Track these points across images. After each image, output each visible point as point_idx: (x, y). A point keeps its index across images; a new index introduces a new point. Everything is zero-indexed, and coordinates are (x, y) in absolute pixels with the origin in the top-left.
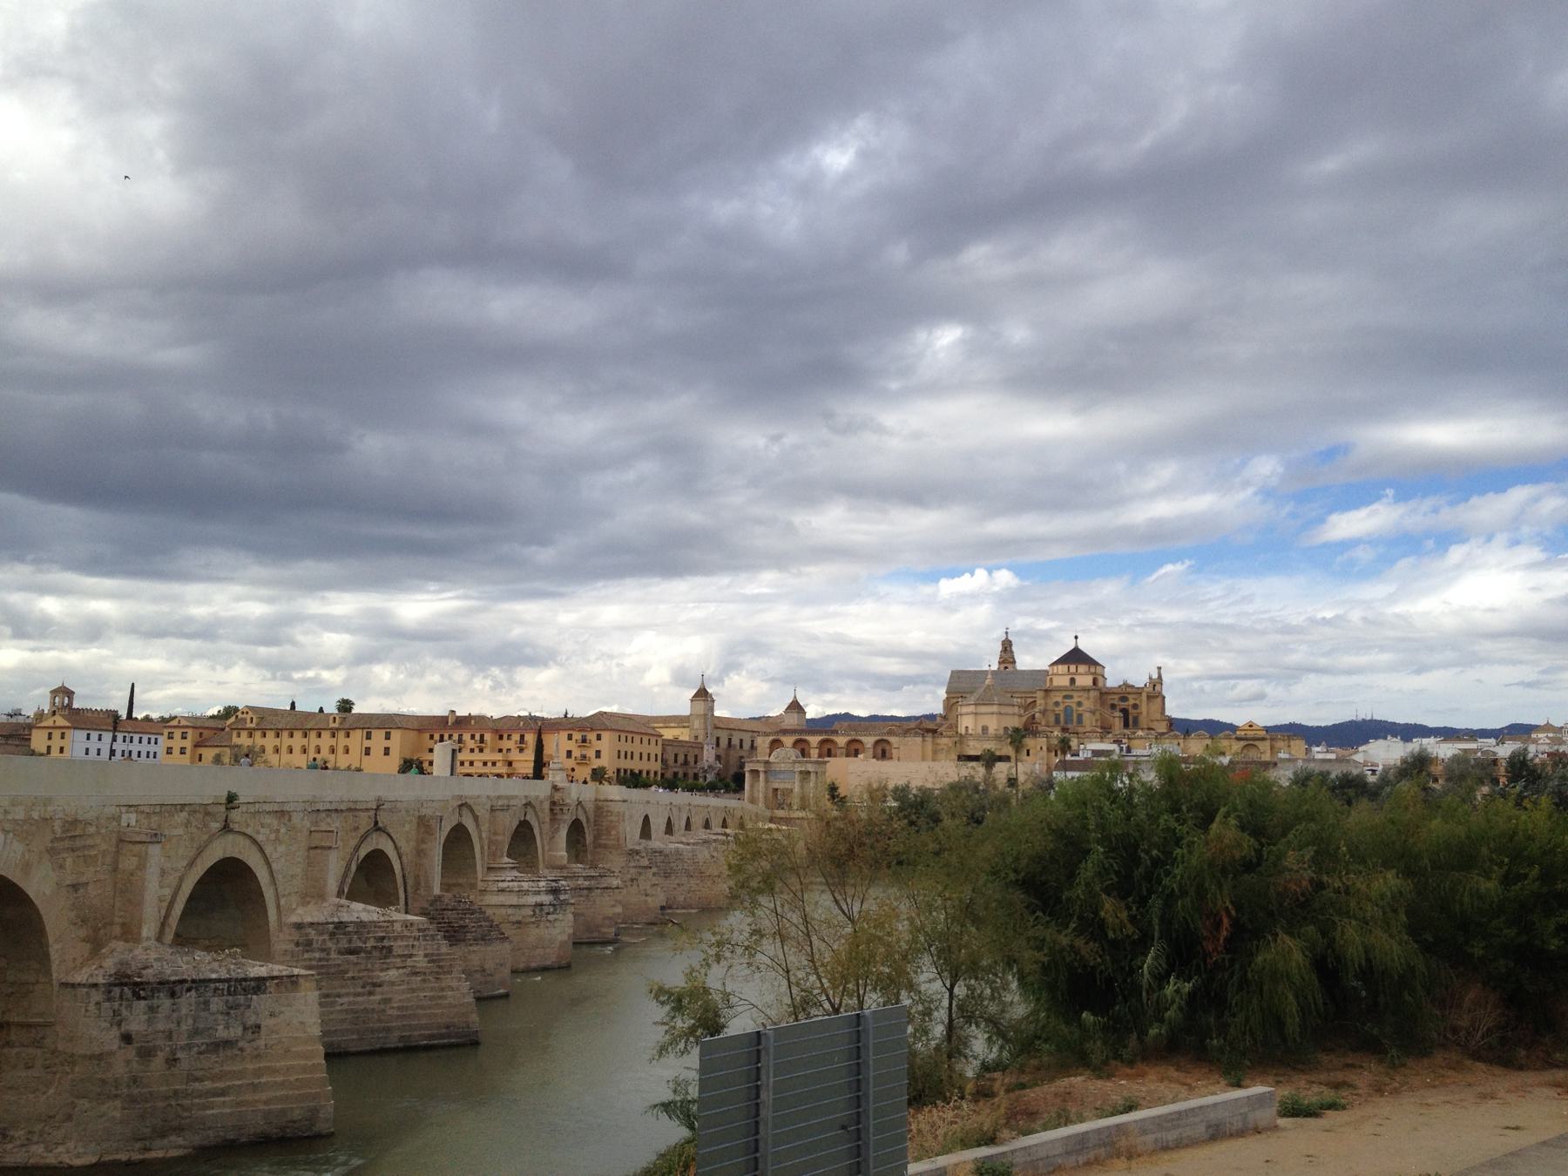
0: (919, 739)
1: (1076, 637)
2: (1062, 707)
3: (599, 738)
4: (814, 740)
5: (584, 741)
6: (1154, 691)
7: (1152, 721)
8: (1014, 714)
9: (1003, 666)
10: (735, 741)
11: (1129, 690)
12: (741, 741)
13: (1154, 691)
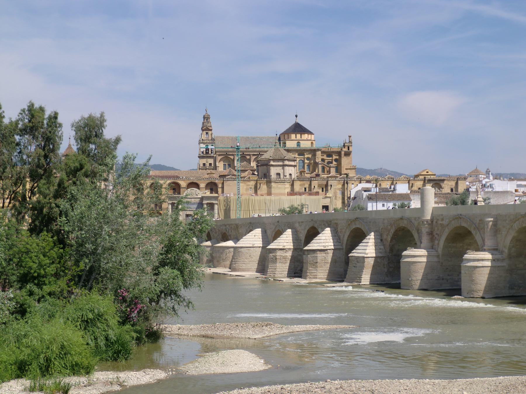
1: (296, 116)
2: (298, 159)
4: (165, 183)
7: (346, 169)
8: (295, 166)
9: (205, 132)
11: (332, 150)
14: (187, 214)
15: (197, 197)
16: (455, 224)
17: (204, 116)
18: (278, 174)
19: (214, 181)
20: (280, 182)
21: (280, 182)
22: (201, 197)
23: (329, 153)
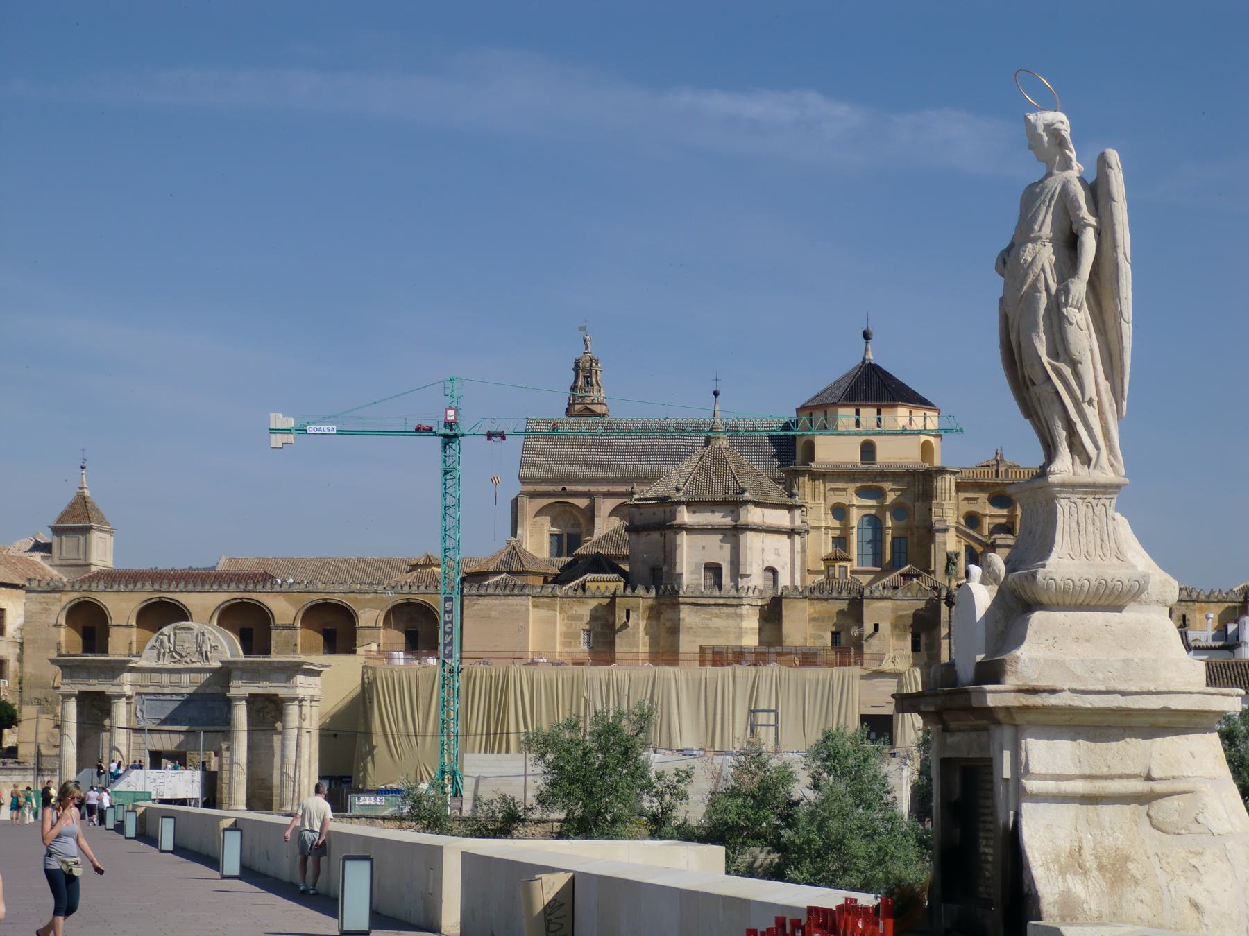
1: (866, 336)
4: (202, 603)
14: (159, 748)
15: (206, 665)
17: (577, 364)
18: (714, 570)
19: (421, 598)
20: (716, 605)
21: (716, 605)
22: (219, 665)
23: (998, 489)
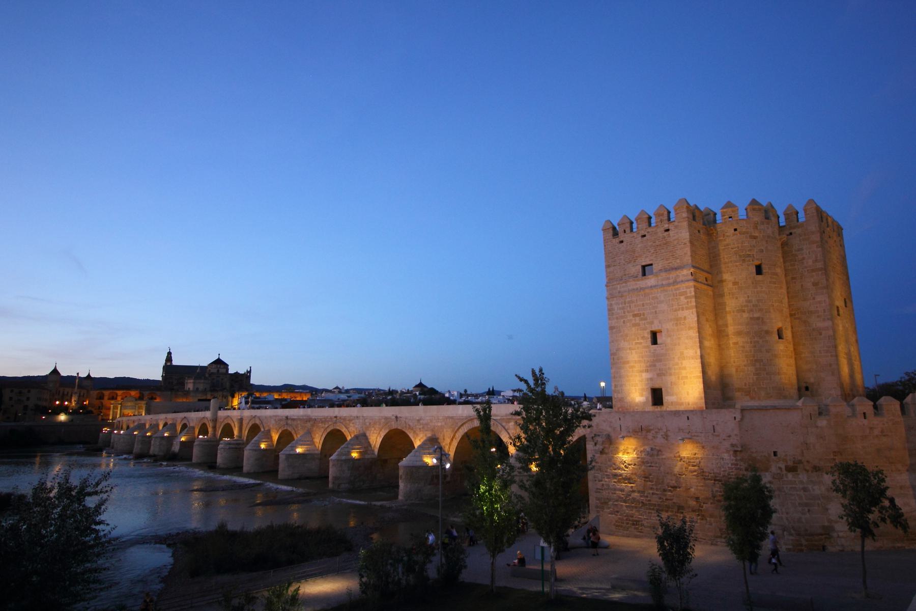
0: (170, 393)
1: (219, 354)
3: (29, 391)
5: (20, 393)
6: (247, 375)
10: (66, 393)
12: (68, 393)
13: (247, 375)
16: (226, 422)
